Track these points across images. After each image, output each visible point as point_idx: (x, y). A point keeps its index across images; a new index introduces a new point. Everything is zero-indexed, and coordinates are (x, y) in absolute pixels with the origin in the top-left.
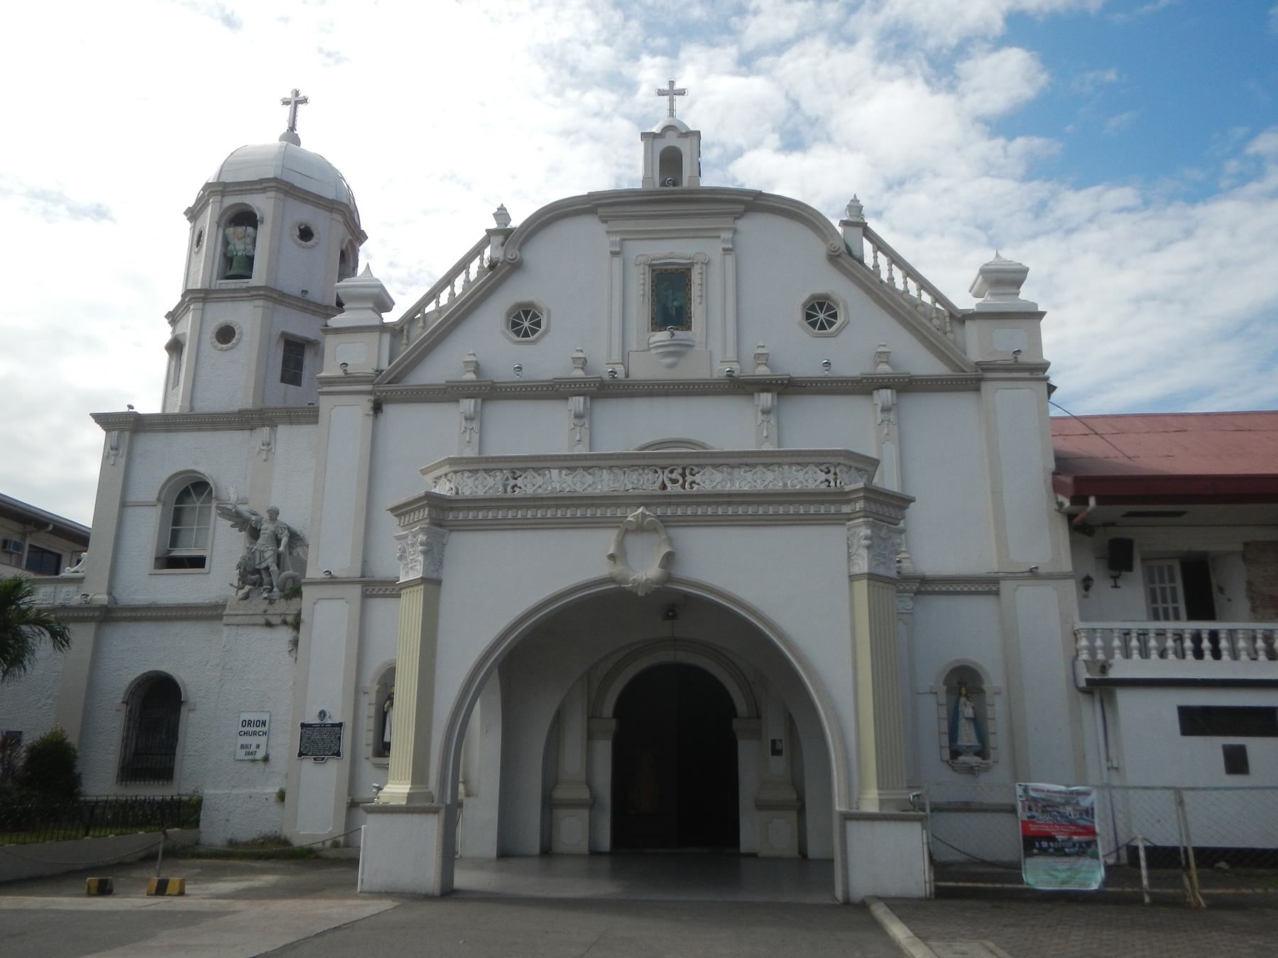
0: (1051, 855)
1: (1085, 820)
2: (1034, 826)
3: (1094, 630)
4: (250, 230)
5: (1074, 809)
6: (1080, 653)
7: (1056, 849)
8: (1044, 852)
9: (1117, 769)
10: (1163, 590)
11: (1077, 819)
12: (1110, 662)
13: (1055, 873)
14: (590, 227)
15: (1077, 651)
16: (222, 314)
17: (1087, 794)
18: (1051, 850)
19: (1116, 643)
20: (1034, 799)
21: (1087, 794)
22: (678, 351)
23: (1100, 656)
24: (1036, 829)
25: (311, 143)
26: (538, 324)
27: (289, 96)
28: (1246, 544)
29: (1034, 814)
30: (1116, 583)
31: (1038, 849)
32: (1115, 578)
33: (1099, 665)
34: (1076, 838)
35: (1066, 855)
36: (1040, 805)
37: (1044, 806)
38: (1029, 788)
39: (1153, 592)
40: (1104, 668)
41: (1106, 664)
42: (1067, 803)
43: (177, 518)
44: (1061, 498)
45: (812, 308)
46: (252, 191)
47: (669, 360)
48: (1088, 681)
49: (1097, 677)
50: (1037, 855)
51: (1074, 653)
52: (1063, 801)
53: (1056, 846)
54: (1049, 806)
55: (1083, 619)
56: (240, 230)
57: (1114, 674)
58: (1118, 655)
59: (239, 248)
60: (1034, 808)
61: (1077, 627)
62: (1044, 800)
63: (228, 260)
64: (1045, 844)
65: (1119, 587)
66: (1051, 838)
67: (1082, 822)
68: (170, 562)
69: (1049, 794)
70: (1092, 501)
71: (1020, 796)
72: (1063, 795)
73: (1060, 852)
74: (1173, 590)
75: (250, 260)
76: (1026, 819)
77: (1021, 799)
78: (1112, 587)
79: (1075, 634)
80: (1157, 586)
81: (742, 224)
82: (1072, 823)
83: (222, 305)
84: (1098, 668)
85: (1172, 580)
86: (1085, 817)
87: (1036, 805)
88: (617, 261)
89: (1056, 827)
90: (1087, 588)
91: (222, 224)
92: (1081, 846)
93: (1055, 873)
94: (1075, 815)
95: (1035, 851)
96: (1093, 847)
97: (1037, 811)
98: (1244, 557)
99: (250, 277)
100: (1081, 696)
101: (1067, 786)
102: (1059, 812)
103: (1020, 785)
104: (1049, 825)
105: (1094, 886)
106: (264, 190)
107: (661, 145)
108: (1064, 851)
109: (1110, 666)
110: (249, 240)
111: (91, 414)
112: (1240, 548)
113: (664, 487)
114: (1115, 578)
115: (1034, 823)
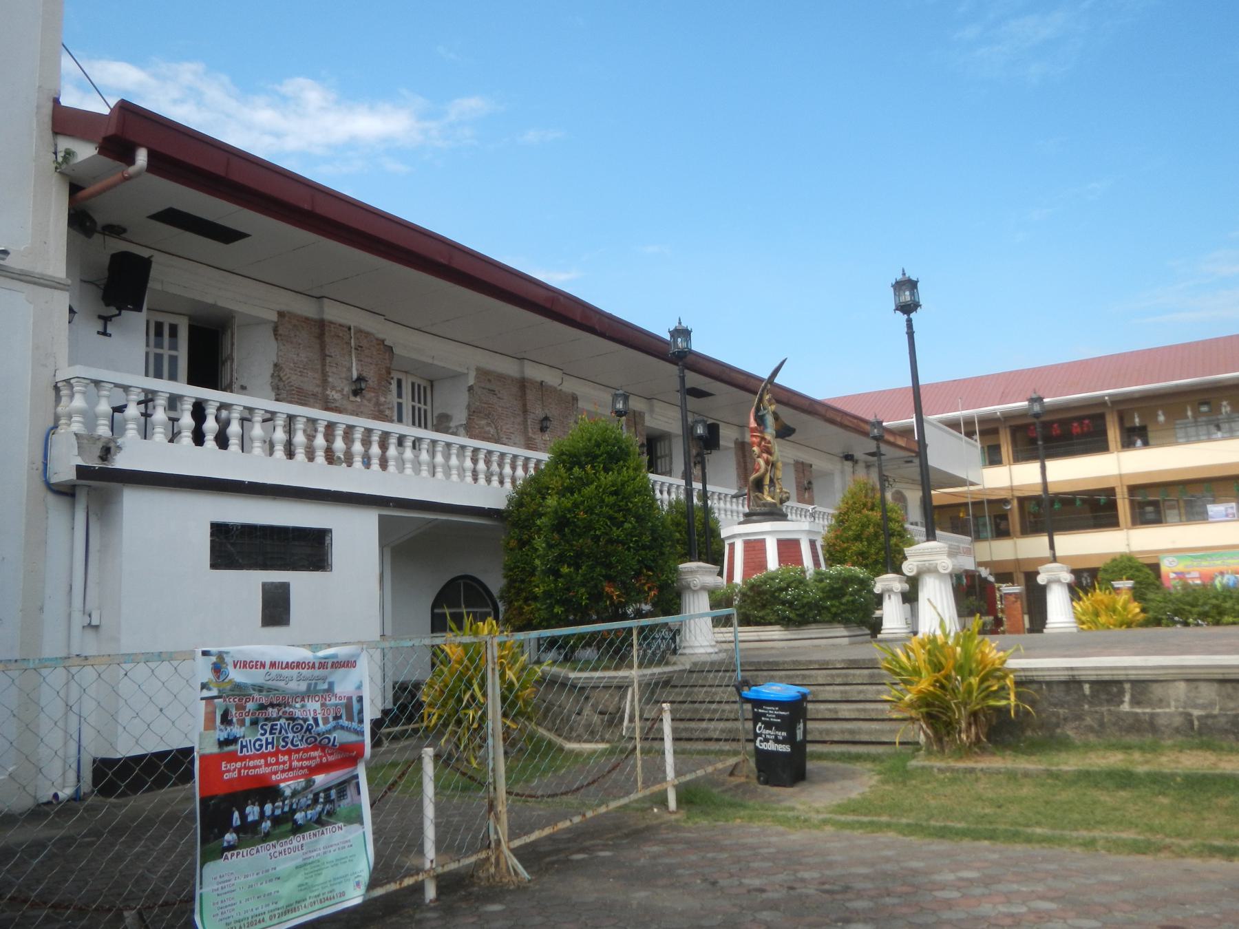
0: (267, 837)
1: (348, 729)
2: (233, 766)
3: (97, 383)
5: (323, 705)
6: (63, 421)
7: (277, 821)
8: (250, 834)
9: (97, 627)
11: (329, 732)
12: (120, 441)
13: (270, 888)
15: (57, 418)
17: (349, 664)
18: (267, 825)
19: (133, 411)
20: (239, 691)
21: (349, 664)
23: (103, 430)
24: (235, 775)
28: (281, 314)
29: (237, 730)
30: (105, 328)
31: (237, 830)
32: (106, 319)
33: (100, 444)
34: (320, 779)
35: (298, 829)
36: (250, 706)
37: (262, 707)
38: (229, 660)
40: (106, 452)
41: (112, 445)
42: (310, 693)
44: (64, 144)
48: (79, 468)
49: (97, 464)
50: (231, 848)
51: (51, 424)
52: (303, 687)
53: (278, 812)
54: (272, 705)
55: (72, 362)
57: (121, 462)
58: (132, 432)
60: (234, 715)
61: (61, 376)
62: (260, 689)
64: (253, 812)
65: (110, 335)
66: (267, 792)
67: (340, 737)
69: (274, 672)
70: (142, 157)
71: (204, 686)
72: (305, 672)
73: (287, 825)
74: (173, 361)
76: (213, 749)
77: (206, 693)
78: (99, 333)
79: (57, 389)
82: (319, 743)
84: (97, 452)
85: (174, 347)
86: (344, 722)
87: (240, 707)
89: (282, 758)
92: (328, 800)
93: (270, 888)
94: (326, 721)
95: (230, 837)
96: (351, 791)
97: (242, 723)
98: (275, 330)
100: (51, 499)
101: (314, 647)
102: (292, 719)
103: (205, 653)
104: (264, 756)
105: (355, 897)
108: (295, 822)
109: (119, 448)
112: (274, 317)
114: (106, 319)
115: (232, 757)
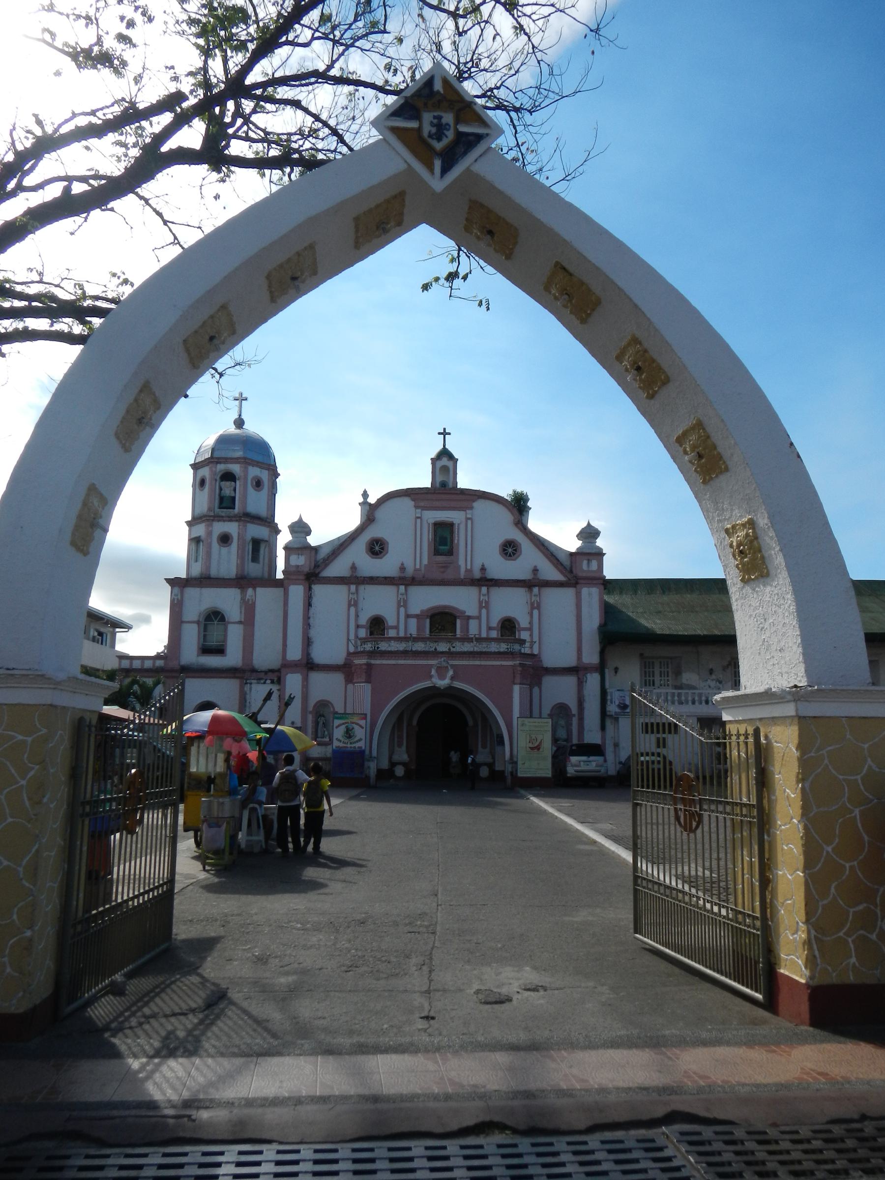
4: (233, 483)
10: (649, 672)
14: (408, 503)
16: (219, 528)
22: (445, 567)
25: (252, 427)
26: (383, 549)
27: (237, 395)
39: (645, 672)
43: (205, 630)
45: (506, 546)
46: (231, 463)
47: (442, 570)
56: (228, 483)
59: (227, 492)
63: (222, 499)
68: (206, 650)
75: (234, 499)
80: (647, 670)
81: (475, 504)
83: (221, 523)
88: (419, 521)
90: (616, 672)
91: (218, 478)
99: (234, 508)
106: (239, 463)
107: (439, 464)
110: (232, 488)
111: (166, 579)
113: (449, 649)
